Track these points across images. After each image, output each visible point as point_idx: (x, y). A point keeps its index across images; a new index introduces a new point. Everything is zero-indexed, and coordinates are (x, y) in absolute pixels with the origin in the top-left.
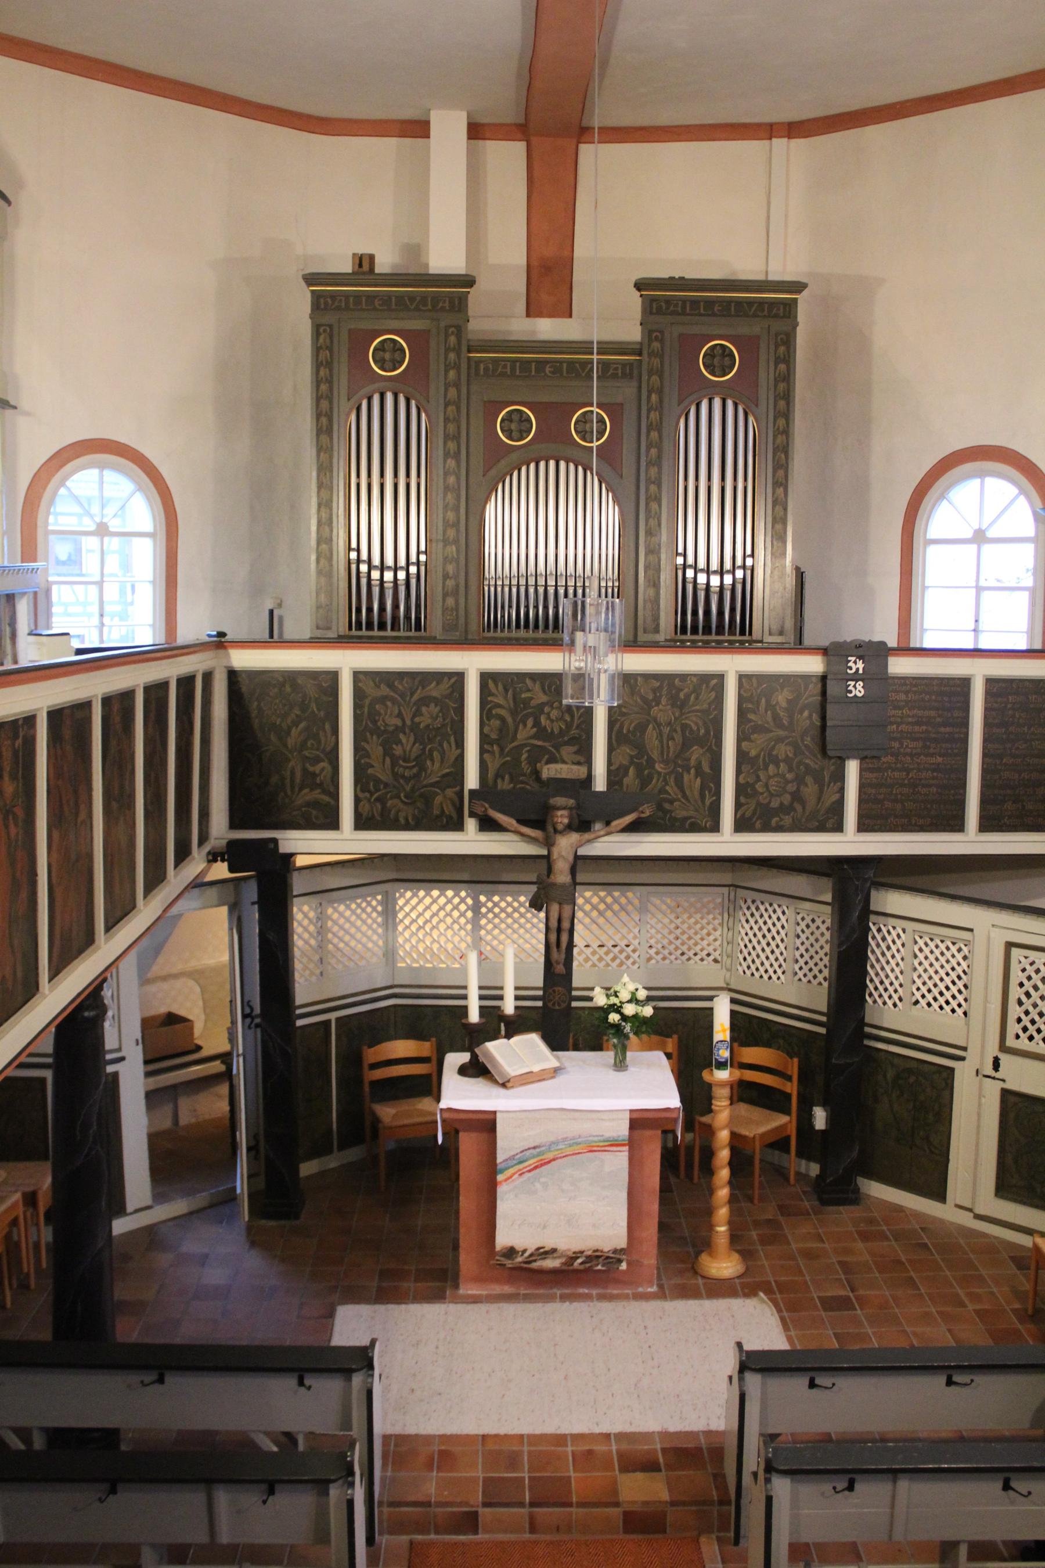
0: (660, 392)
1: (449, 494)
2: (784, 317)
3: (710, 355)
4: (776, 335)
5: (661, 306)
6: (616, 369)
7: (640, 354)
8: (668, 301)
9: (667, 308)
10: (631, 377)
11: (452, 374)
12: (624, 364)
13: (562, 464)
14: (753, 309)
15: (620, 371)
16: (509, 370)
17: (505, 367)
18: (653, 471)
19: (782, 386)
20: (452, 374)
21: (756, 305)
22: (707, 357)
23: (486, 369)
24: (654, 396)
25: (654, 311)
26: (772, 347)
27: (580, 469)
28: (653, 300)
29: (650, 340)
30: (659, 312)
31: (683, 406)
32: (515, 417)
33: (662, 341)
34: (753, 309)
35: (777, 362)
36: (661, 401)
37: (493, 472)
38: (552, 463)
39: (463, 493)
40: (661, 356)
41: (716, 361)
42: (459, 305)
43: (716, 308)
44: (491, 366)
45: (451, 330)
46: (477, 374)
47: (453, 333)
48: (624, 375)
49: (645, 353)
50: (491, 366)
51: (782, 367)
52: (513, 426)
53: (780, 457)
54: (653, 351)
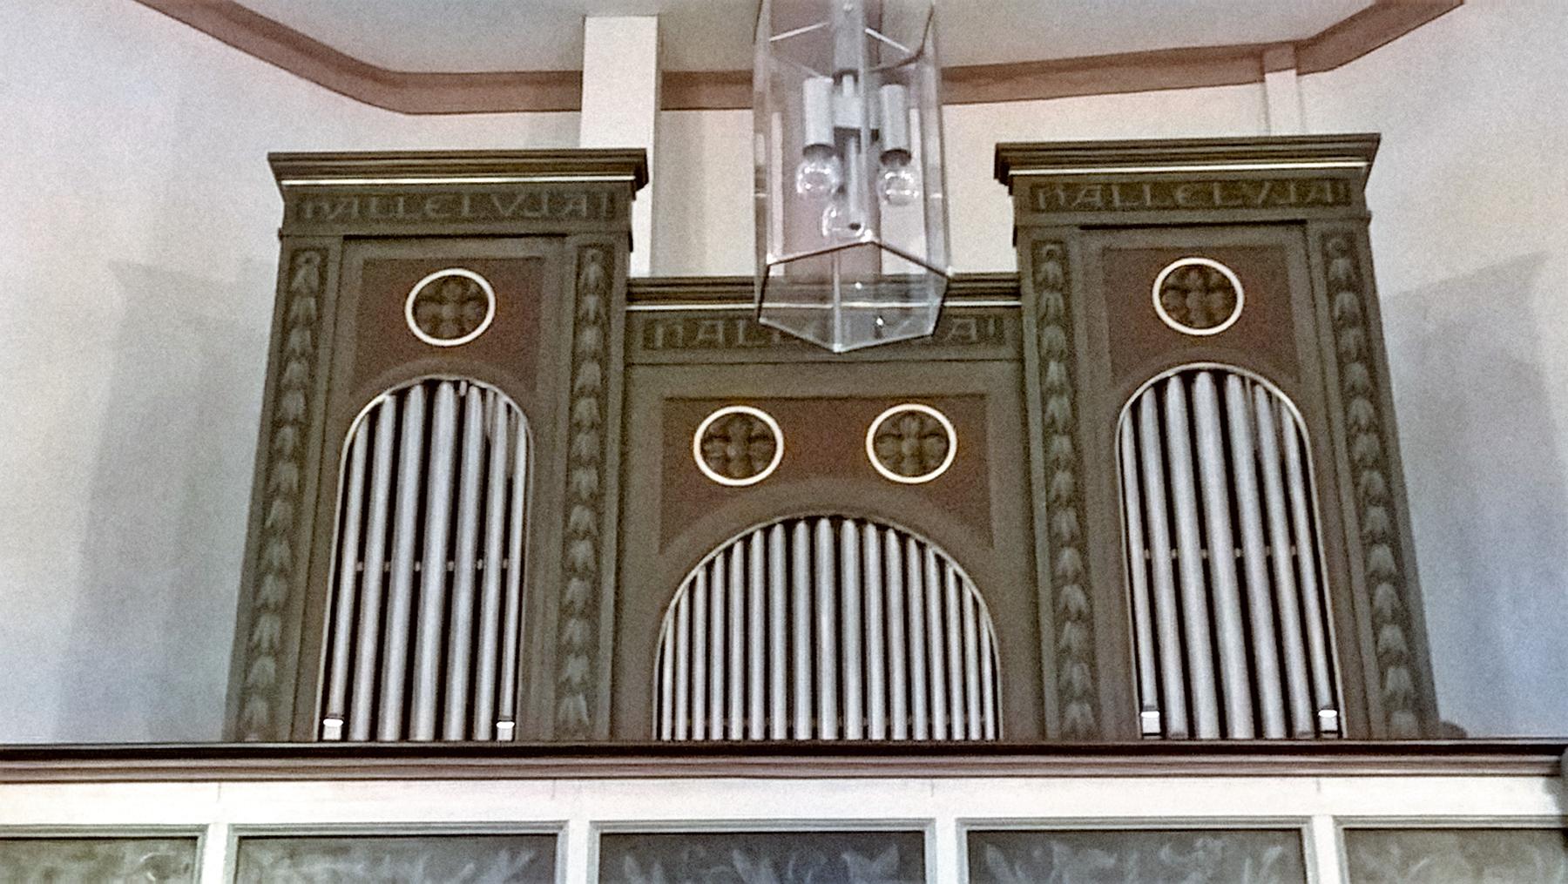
0: (1069, 358)
1: (575, 584)
2: (1335, 203)
3: (1177, 289)
4: (1324, 238)
5: (1057, 198)
6: (965, 327)
7: (1016, 293)
8: (1072, 186)
9: (1073, 199)
10: (999, 339)
11: (590, 337)
12: (982, 318)
13: (849, 527)
14: (1264, 192)
15: (973, 332)
16: (720, 337)
17: (713, 329)
18: (1068, 557)
19: (1351, 337)
20: (590, 337)
21: (1267, 185)
22: (1170, 293)
23: (670, 334)
24: (1053, 367)
25: (1043, 206)
26: (1316, 259)
27: (892, 538)
28: (1036, 185)
29: (1036, 263)
30: (1053, 206)
31: (1126, 385)
32: (737, 430)
33: (1064, 259)
34: (1264, 192)
35: (1333, 288)
36: (1071, 375)
37: (682, 542)
38: (824, 527)
39: (609, 581)
40: (1063, 287)
41: (1192, 300)
42: (615, 208)
43: (1180, 196)
44: (680, 329)
45: (591, 252)
46: (649, 341)
47: (593, 259)
48: (983, 337)
49: (1027, 286)
50: (680, 329)
51: (1346, 299)
52: (732, 451)
53: (1371, 482)
54: (1046, 279)
